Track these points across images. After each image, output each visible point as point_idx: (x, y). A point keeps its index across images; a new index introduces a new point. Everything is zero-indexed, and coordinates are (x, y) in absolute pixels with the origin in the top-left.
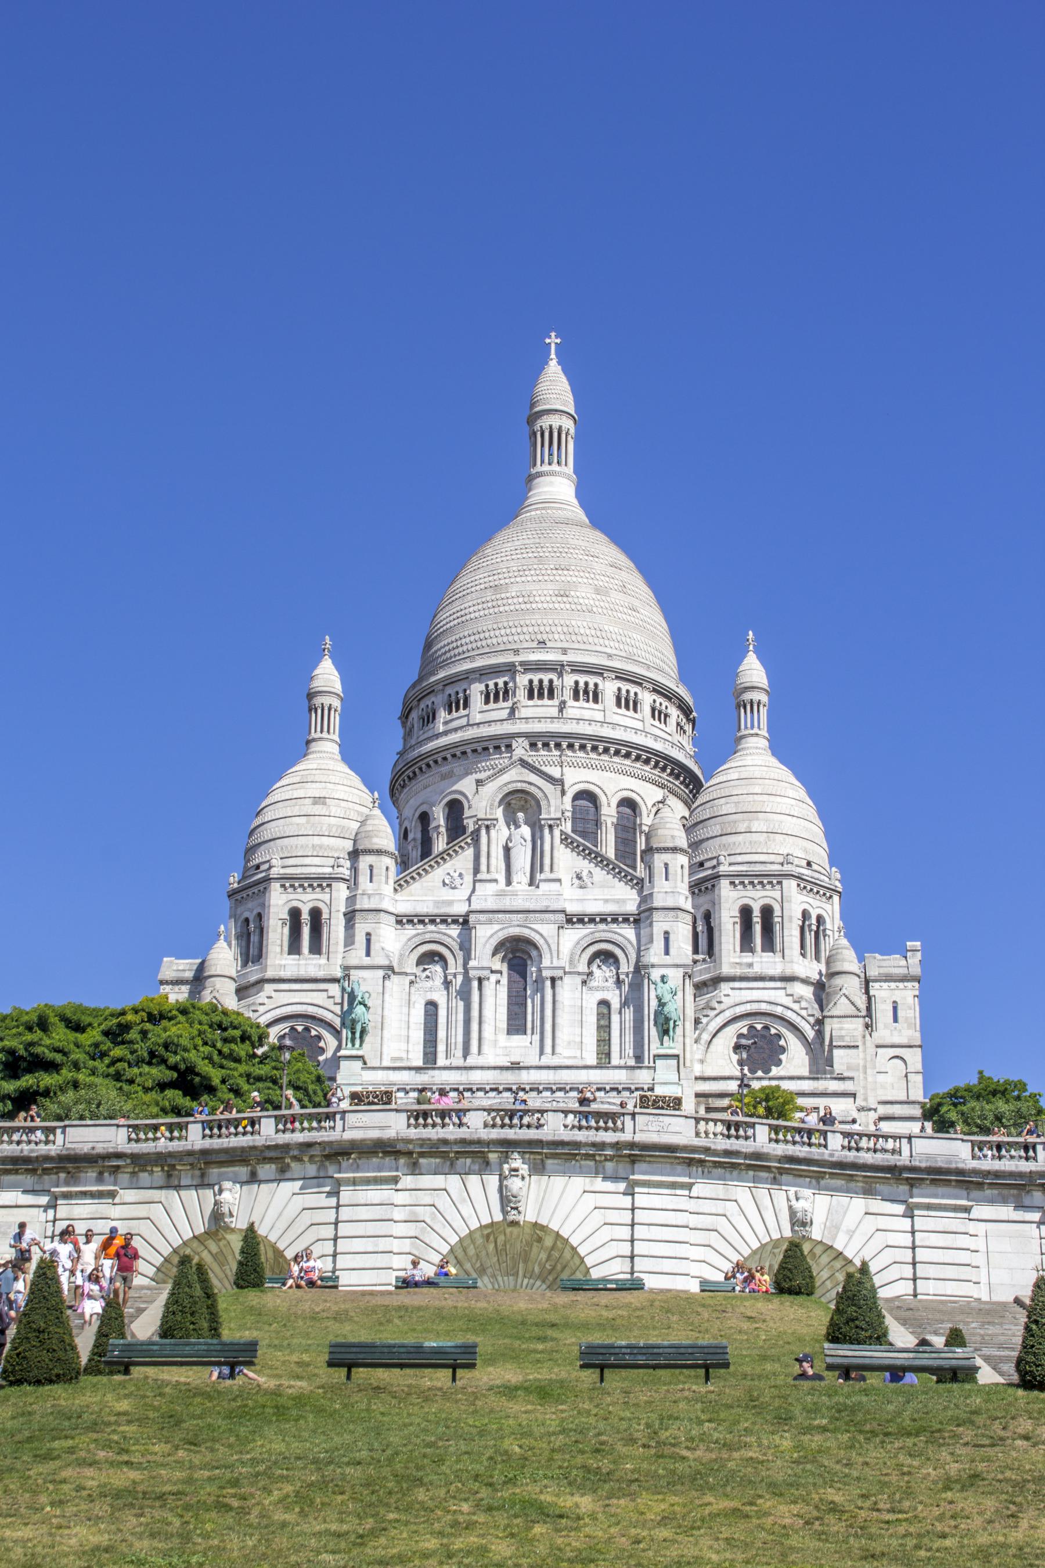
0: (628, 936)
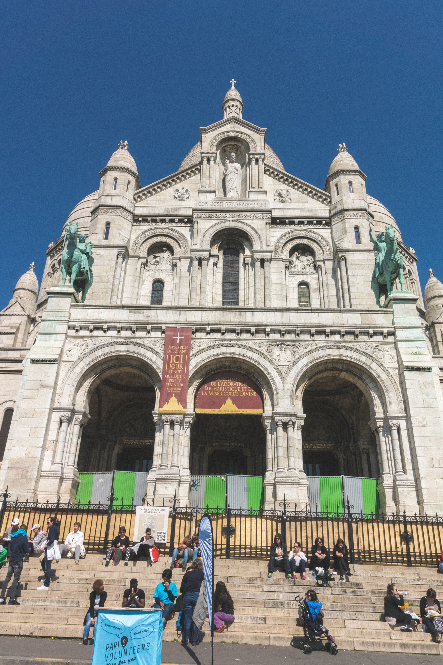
0: (322, 234)
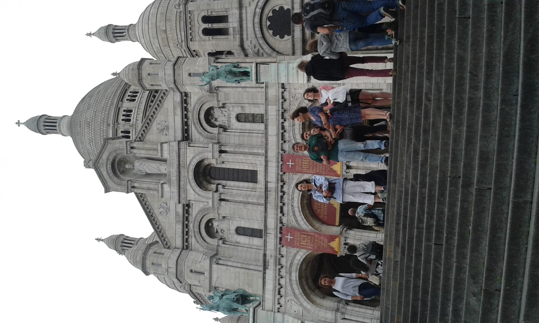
0: (195, 100)
